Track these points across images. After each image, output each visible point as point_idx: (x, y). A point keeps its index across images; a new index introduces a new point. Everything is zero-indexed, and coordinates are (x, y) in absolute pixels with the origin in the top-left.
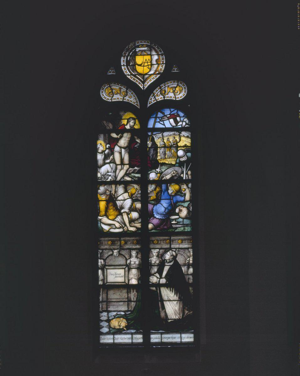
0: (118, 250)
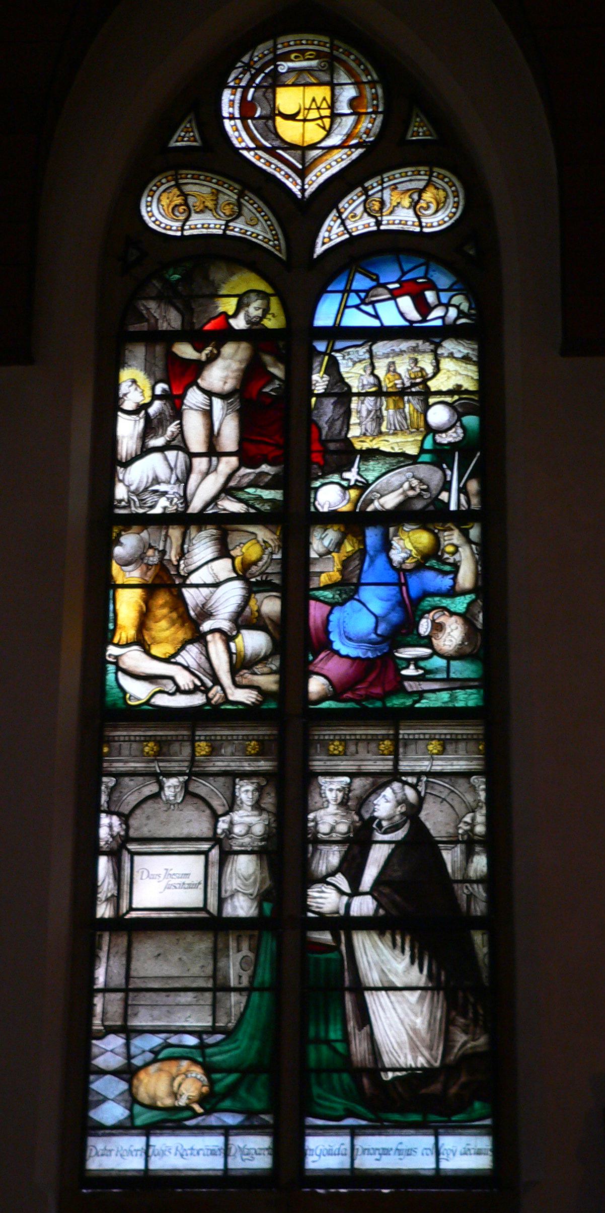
0: (181, 779)
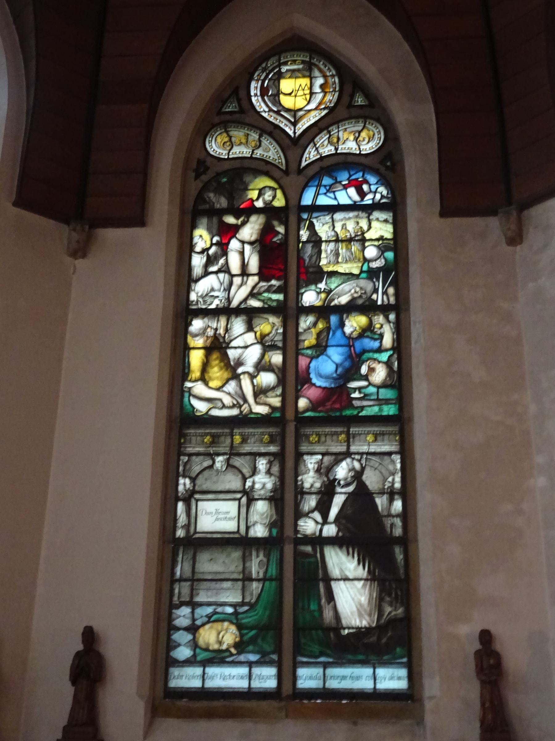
0: (226, 457)
